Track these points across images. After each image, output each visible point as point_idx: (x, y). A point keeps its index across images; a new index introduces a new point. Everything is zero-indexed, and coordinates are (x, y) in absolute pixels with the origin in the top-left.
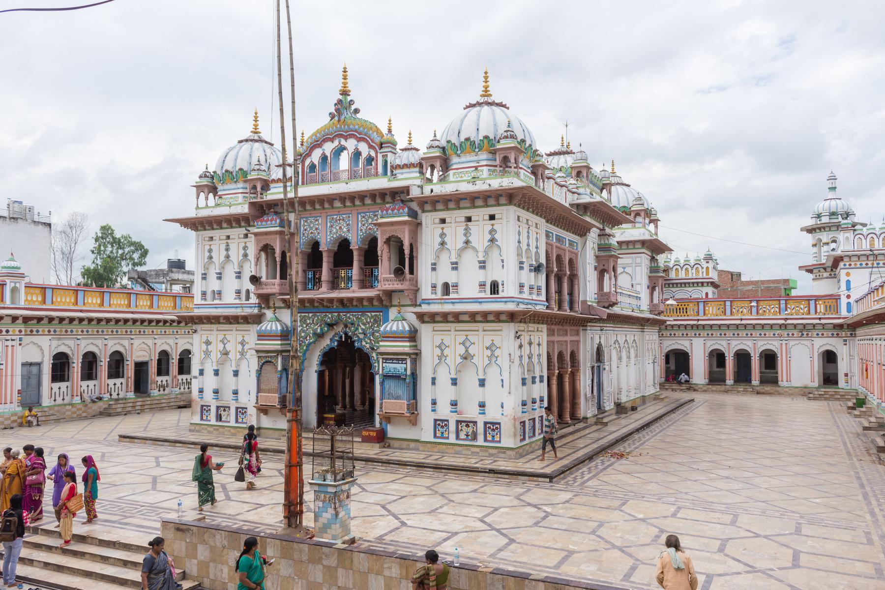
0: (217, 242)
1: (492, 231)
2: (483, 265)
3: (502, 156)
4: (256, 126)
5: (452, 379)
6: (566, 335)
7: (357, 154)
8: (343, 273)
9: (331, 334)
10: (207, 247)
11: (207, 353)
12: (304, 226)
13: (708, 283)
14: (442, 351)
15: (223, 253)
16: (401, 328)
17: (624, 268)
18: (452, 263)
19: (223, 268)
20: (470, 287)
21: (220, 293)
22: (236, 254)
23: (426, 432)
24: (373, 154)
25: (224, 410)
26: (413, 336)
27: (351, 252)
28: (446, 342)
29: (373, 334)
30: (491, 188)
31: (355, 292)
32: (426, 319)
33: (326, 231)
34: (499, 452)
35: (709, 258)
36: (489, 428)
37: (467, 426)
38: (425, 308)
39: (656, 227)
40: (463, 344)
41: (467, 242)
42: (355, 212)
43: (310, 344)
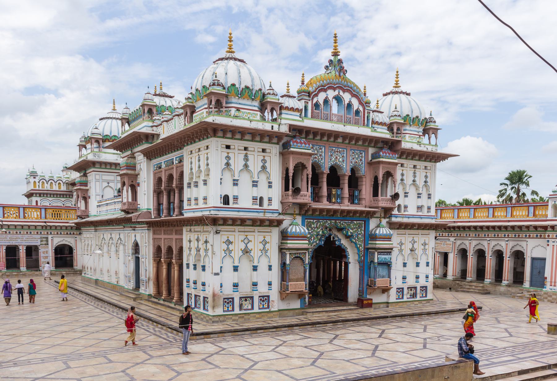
0: (236, 152)
8: (334, 191)
21: (236, 198)
25: (246, 300)
31: (346, 206)
38: (394, 219)
41: (414, 181)
42: (349, 148)
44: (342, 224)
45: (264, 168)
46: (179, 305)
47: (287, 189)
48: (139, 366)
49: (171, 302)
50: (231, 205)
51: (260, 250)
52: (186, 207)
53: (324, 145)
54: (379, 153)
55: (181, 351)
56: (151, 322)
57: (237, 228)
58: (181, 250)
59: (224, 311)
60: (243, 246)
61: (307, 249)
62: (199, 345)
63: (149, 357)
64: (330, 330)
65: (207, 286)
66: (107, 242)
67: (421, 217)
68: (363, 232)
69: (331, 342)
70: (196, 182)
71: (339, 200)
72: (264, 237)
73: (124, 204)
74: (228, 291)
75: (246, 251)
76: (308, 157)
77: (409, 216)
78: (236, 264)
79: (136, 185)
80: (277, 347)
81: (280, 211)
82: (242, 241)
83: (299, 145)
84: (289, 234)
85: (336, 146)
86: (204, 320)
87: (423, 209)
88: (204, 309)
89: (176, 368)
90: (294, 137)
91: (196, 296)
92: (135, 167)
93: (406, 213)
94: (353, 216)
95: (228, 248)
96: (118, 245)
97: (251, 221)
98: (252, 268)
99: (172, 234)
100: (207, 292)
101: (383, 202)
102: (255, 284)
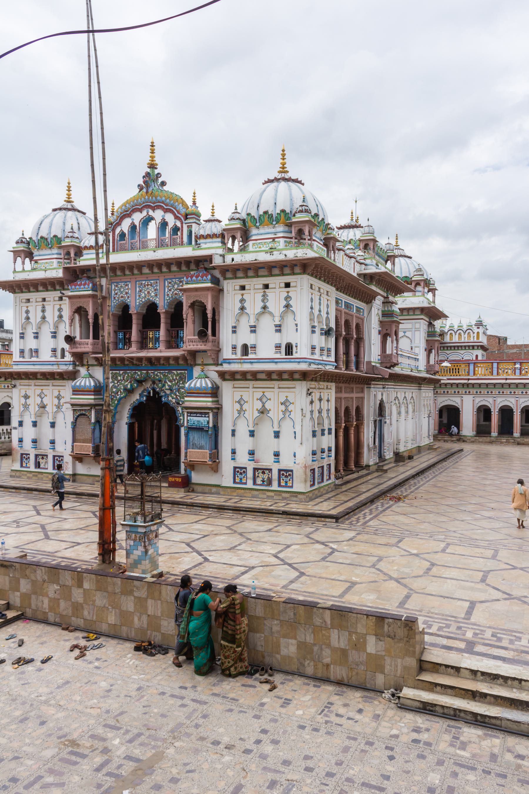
0: (34, 304)
1: (288, 298)
2: (279, 329)
3: (297, 229)
4: (69, 195)
5: (250, 431)
6: (352, 392)
7: (164, 224)
8: (151, 334)
9: (140, 390)
10: (24, 309)
11: (26, 406)
12: (115, 290)
13: (478, 346)
14: (241, 406)
15: (40, 314)
16: (204, 385)
17: (405, 332)
18: (251, 327)
19: (40, 328)
20: (266, 347)
21: (37, 351)
22: (51, 315)
23: (226, 478)
24: (179, 224)
25: (43, 458)
26: (215, 392)
27: (159, 314)
28: (245, 398)
29: (179, 390)
30: (287, 259)
31: (162, 352)
32: (227, 377)
33: (135, 295)
34: (291, 496)
35: (479, 324)
36: (283, 474)
37: (263, 473)
38: (226, 367)
39: (434, 295)
40: (260, 399)
41: (265, 307)
42: (162, 278)
43: (121, 399)
53: (129, 280)
72: (59, 391)
83: (77, 287)
85: (145, 279)
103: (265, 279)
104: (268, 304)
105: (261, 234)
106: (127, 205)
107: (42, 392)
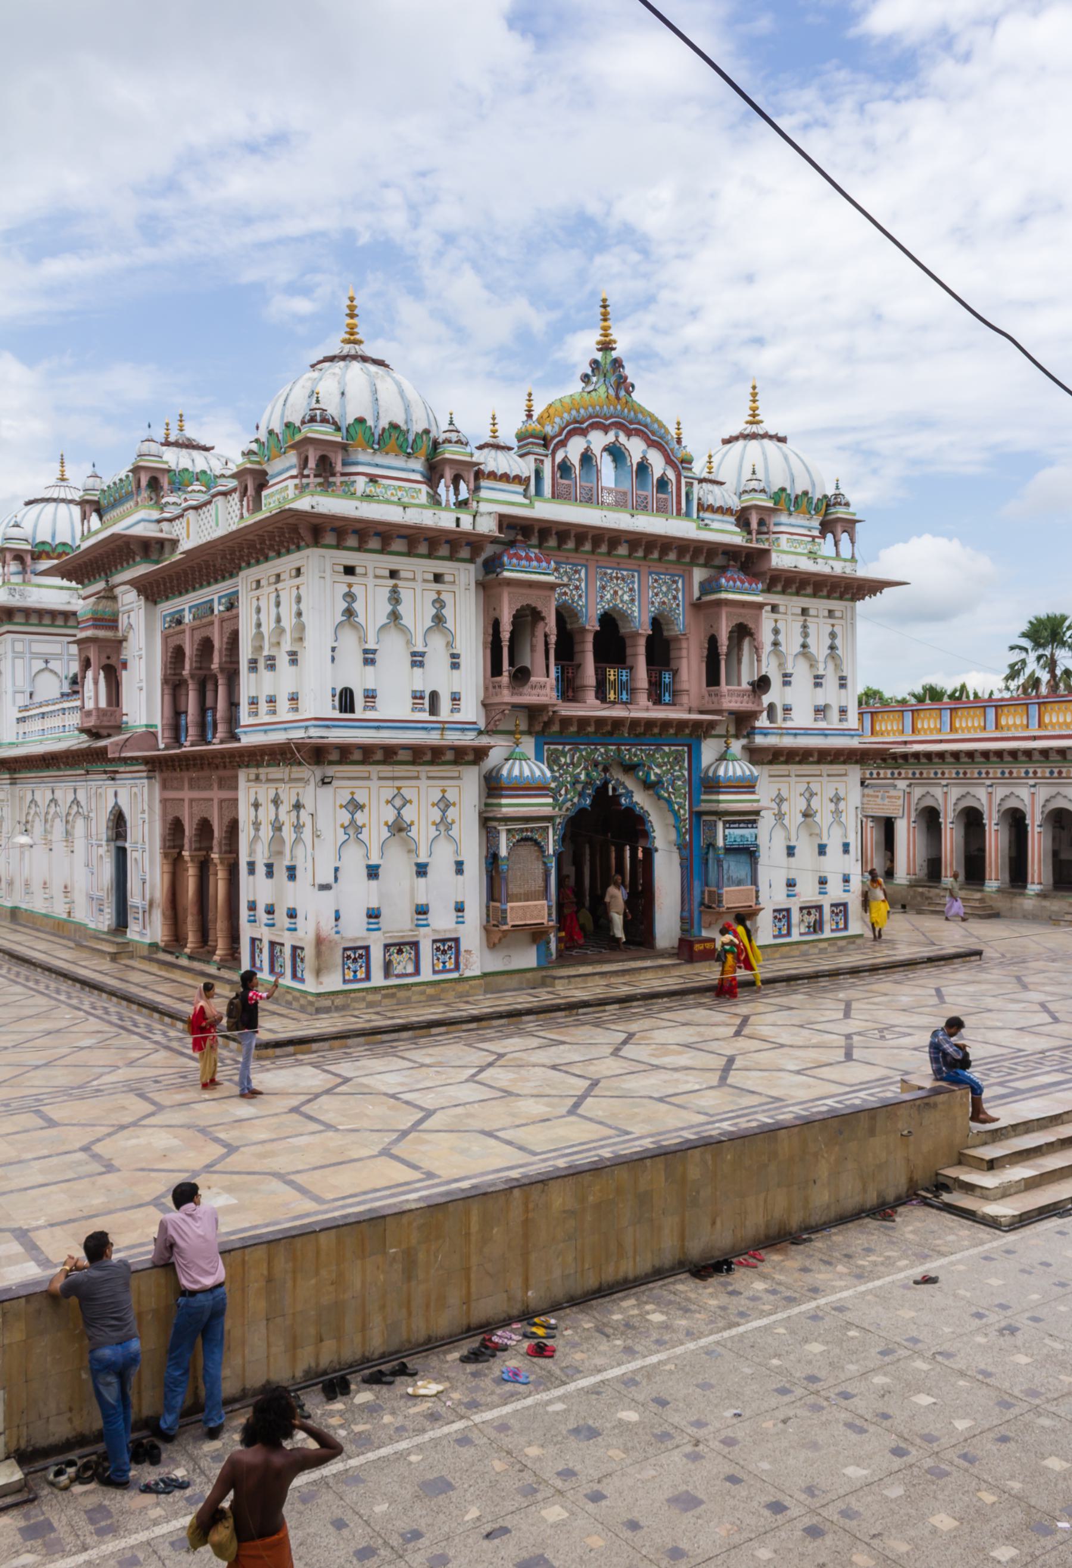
0: (370, 581)
1: (833, 635)
4: (352, 330)
8: (612, 674)
16: (748, 773)
21: (370, 696)
24: (671, 475)
31: (644, 710)
37: (809, 913)
38: (759, 740)
41: (804, 646)
42: (644, 570)
44: (635, 755)
45: (439, 619)
46: (230, 968)
47: (496, 669)
48: (126, 1133)
49: (208, 962)
50: (359, 713)
51: (434, 823)
52: (245, 718)
54: (717, 580)
55: (237, 1090)
56: (156, 1015)
57: (374, 770)
58: (233, 828)
59: (345, 981)
60: (390, 815)
61: (549, 819)
62: (283, 1072)
63: (152, 1108)
64: (613, 1022)
65: (300, 919)
66: (42, 810)
67: (823, 733)
68: (686, 773)
69: (616, 1052)
70: (272, 658)
71: (624, 697)
72: (444, 791)
73: (88, 714)
74: (355, 928)
75: (399, 828)
76: (547, 593)
77: (796, 732)
78: (374, 860)
79: (119, 667)
80: (482, 1069)
81: (482, 725)
82: (388, 802)
83: (524, 562)
84: (504, 783)
86: (295, 1005)
87: (828, 713)
88: (294, 976)
89: (222, 1136)
90: (512, 544)
91: (272, 944)
92: (116, 621)
93: (789, 724)
94: (660, 734)
95: (353, 821)
96: (70, 818)
97: (410, 752)
98: (414, 869)
99: (210, 787)
100: (300, 933)
101: (732, 697)
102: (422, 911)
103: (807, 599)
104: (809, 641)
105: (377, 465)
106: (582, 411)
107: (399, 794)
